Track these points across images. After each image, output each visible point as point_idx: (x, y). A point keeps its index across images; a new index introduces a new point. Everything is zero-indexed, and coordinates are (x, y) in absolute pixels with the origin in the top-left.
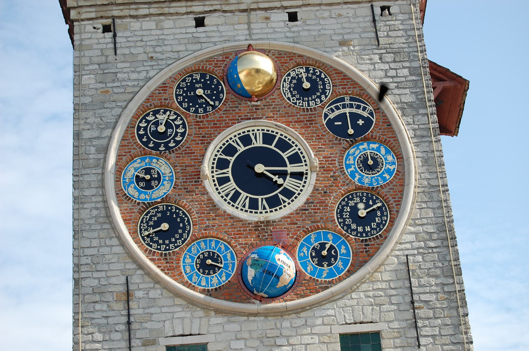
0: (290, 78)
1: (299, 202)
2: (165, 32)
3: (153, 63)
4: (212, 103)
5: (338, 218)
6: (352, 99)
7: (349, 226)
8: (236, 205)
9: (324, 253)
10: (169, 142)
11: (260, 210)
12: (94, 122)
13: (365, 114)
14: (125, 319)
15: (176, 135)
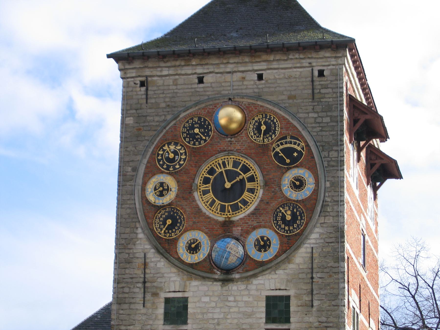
0: (254, 121)
1: (252, 208)
2: (179, 87)
3: (168, 110)
4: (204, 138)
5: (274, 221)
6: (292, 137)
7: (280, 226)
8: (212, 209)
9: (262, 243)
10: (176, 164)
11: (226, 213)
12: (131, 150)
13: (299, 149)
14: (142, 280)
15: (180, 160)
